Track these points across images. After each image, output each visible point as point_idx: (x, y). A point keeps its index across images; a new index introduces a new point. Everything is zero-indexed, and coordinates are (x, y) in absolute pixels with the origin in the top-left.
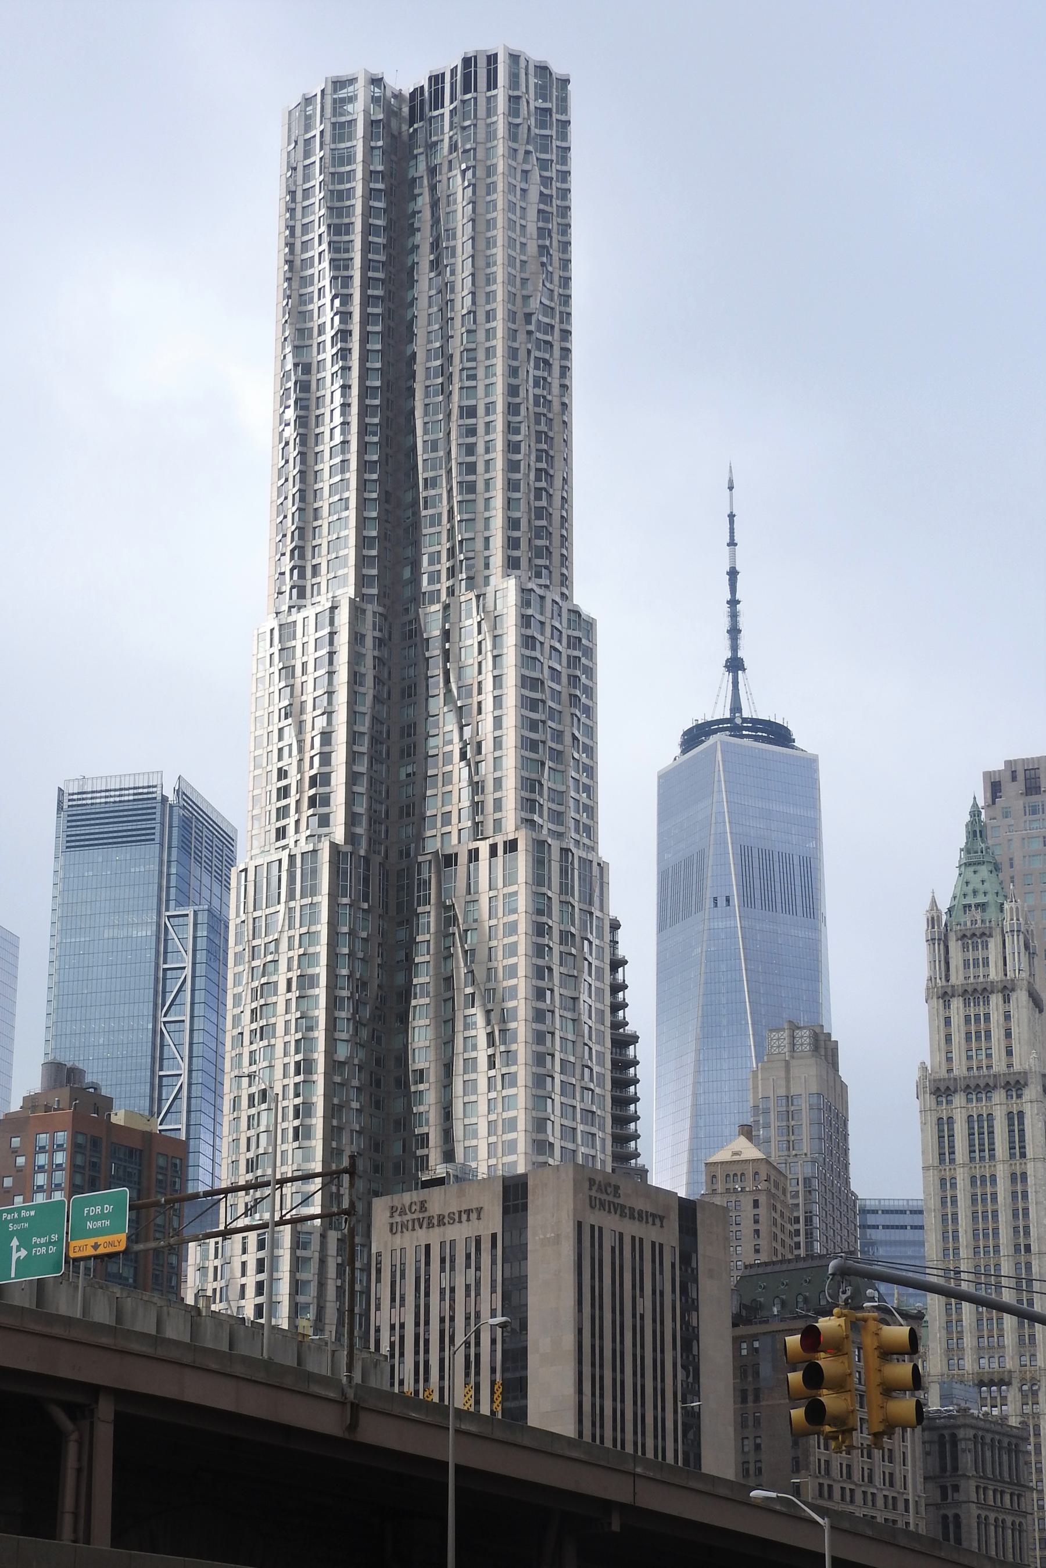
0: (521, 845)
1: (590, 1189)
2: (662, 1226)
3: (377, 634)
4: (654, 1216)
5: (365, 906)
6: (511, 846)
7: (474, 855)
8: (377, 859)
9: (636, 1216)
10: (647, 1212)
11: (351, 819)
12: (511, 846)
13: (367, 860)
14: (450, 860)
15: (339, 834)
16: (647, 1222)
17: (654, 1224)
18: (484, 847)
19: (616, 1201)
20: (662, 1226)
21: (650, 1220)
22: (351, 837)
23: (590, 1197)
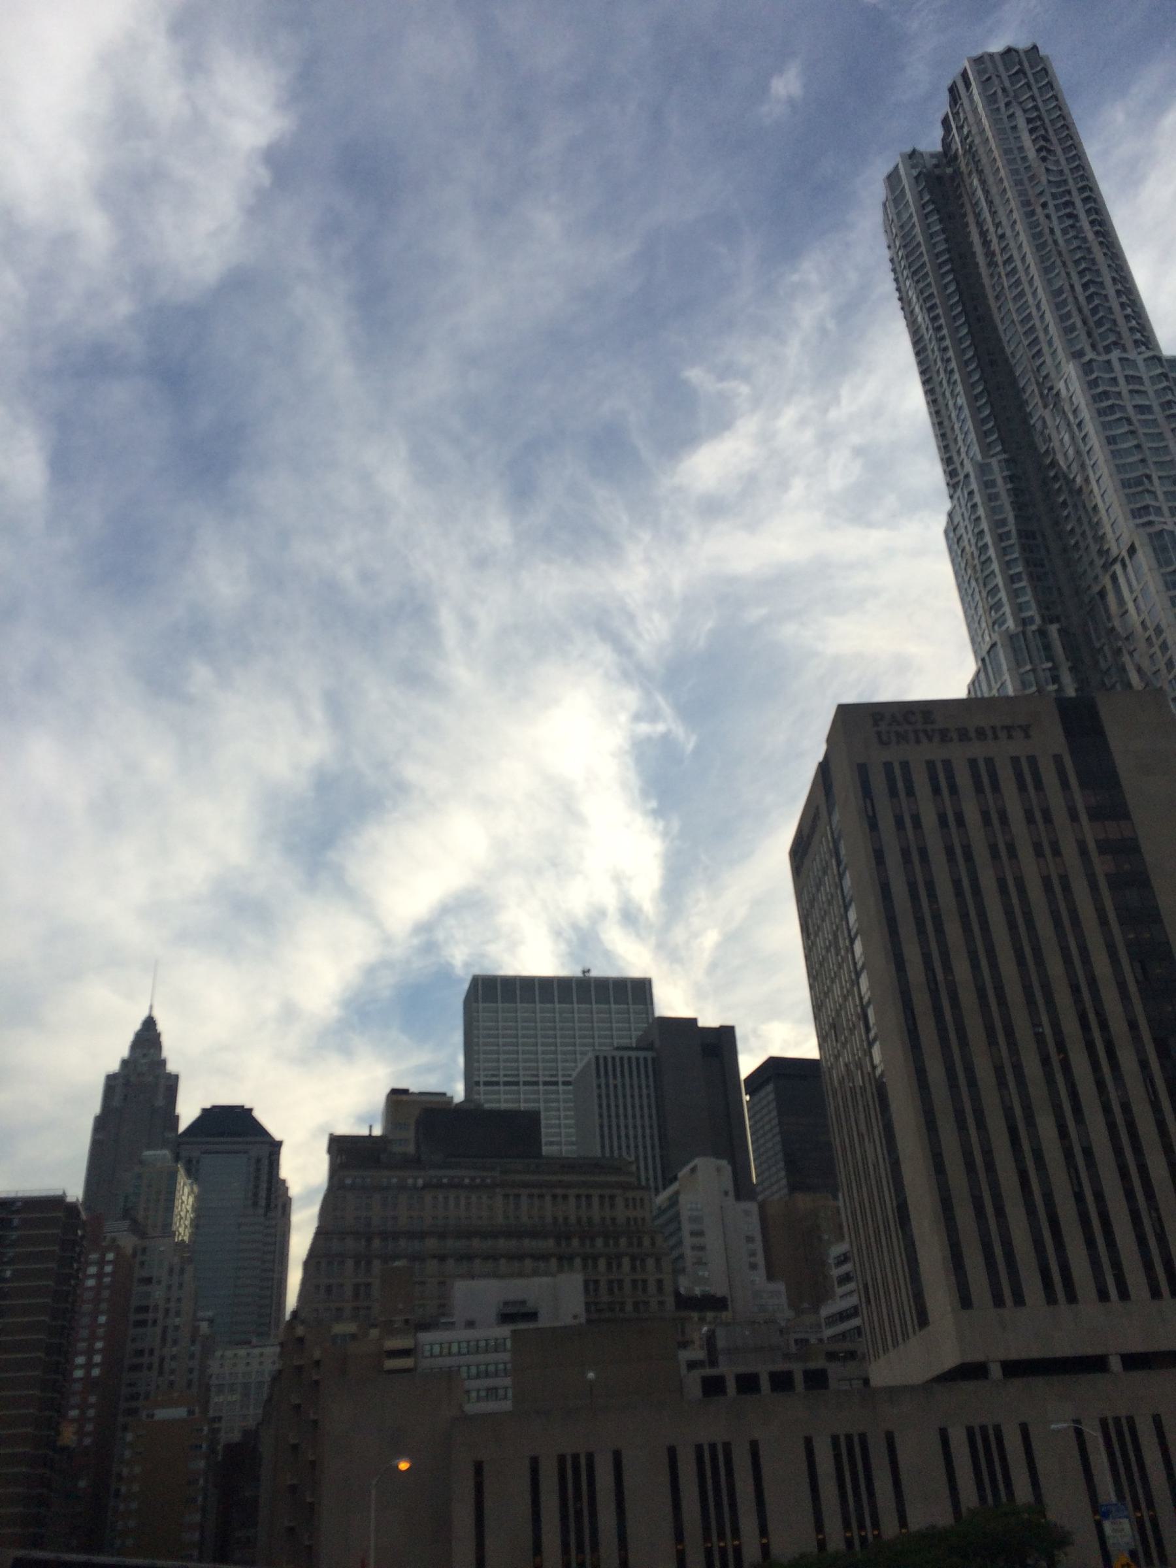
0: (1137, 545)
1: (876, 724)
2: (1027, 736)
3: (1006, 473)
4: (1008, 728)
5: (1050, 665)
6: (1132, 550)
7: (1114, 578)
8: (1053, 629)
9: (972, 734)
10: (993, 728)
11: (1018, 608)
12: (1132, 550)
13: (1042, 633)
14: (1102, 594)
15: (1010, 623)
16: (996, 738)
17: (1010, 737)
18: (1118, 567)
19: (929, 727)
20: (1027, 736)
21: (1002, 735)
22: (1025, 622)
23: (879, 734)
